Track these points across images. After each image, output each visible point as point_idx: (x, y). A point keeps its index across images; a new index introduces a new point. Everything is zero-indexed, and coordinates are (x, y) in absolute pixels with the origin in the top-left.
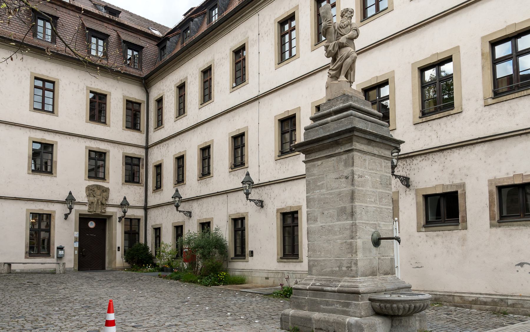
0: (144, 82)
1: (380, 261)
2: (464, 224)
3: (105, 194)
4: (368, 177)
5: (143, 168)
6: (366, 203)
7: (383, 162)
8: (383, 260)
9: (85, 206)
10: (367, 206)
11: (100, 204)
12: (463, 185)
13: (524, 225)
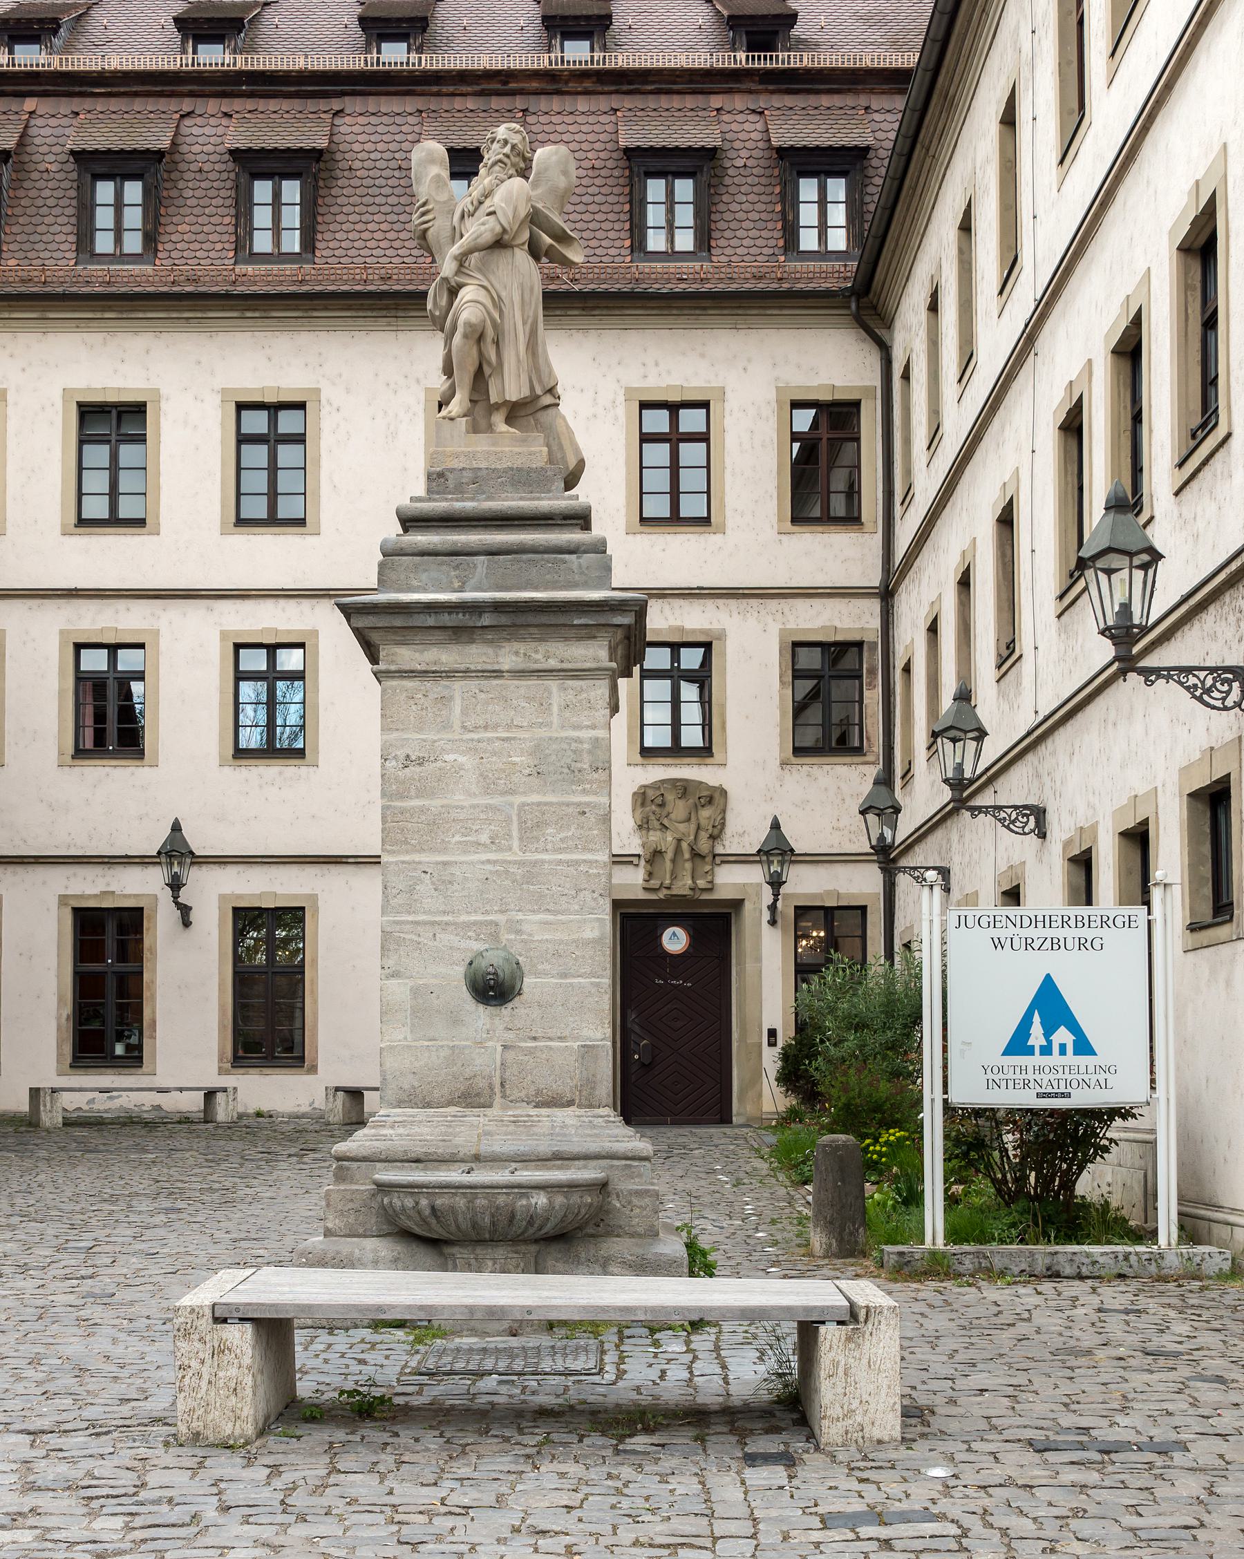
0: (853, 306)
1: (510, 1055)
3: (705, 813)
4: (462, 759)
5: (872, 686)
6: (445, 850)
7: (554, 690)
8: (530, 1052)
9: (631, 868)
10: (445, 864)
11: (687, 856)
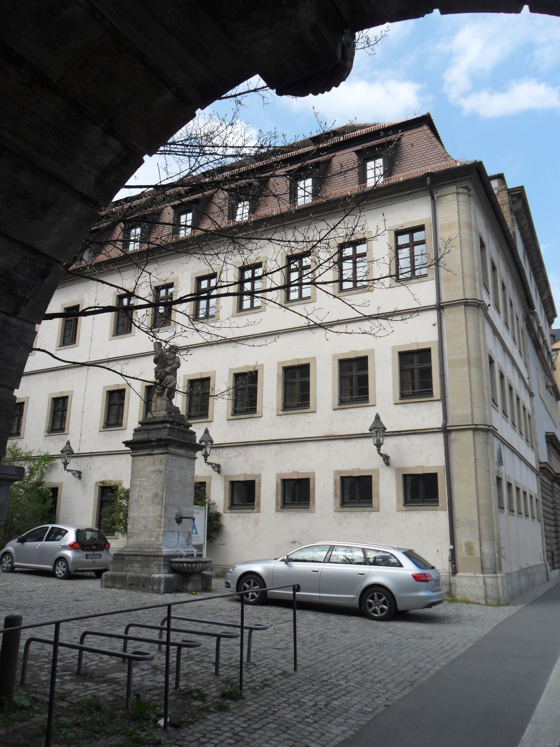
2: (258, 508)
12: (259, 476)
13: (297, 512)
